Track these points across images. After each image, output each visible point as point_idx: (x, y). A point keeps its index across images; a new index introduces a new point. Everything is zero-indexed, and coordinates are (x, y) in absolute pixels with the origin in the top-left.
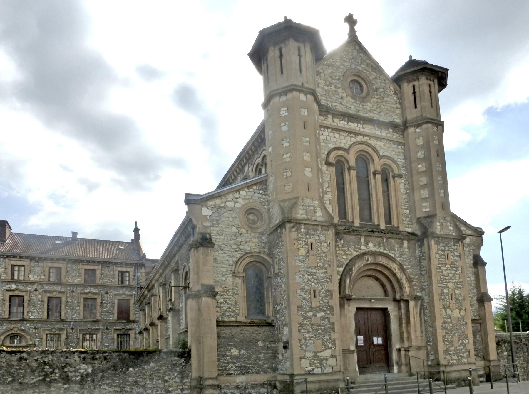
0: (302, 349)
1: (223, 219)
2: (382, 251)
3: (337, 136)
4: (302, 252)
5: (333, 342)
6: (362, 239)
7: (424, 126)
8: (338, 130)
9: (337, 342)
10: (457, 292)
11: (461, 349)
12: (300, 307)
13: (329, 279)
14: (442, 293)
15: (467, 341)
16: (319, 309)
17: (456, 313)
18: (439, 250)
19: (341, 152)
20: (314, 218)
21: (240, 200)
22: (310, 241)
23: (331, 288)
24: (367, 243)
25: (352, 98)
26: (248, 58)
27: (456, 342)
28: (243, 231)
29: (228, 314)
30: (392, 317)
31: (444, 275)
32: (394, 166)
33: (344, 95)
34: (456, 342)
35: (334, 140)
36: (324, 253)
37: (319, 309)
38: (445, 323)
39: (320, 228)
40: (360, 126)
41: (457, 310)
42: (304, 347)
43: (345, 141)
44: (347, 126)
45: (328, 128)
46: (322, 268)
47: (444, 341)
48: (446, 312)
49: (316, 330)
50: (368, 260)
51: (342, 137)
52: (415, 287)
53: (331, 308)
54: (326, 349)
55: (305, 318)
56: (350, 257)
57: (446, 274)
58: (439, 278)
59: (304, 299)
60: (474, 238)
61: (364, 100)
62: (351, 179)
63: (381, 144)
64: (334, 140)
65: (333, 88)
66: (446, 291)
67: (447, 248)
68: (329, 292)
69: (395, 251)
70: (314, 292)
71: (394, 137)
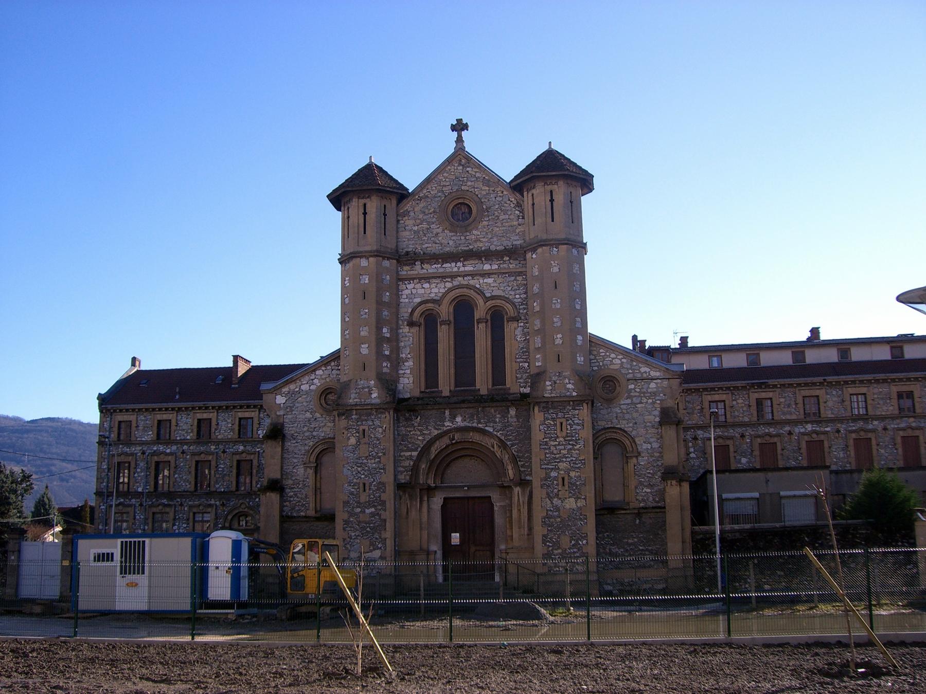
0: (347, 549)
1: (297, 405)
2: (475, 425)
3: (426, 285)
4: (353, 441)
5: (384, 541)
6: (447, 412)
7: (540, 250)
8: (427, 278)
9: (388, 542)
10: (572, 474)
11: (574, 552)
12: (346, 503)
13: (383, 469)
14: (547, 477)
15: (584, 542)
16: (370, 504)
17: (571, 504)
18: (546, 419)
19: (430, 306)
20: (368, 401)
21: (316, 381)
22: (361, 428)
23: (384, 478)
24: (453, 418)
25: (451, 231)
26: (96, 403)
27: (565, 541)
28: (318, 415)
29: (297, 508)
30: (496, 508)
31: (552, 453)
32: (508, 307)
33: (440, 230)
34: (565, 541)
35: (421, 291)
36: (378, 440)
37: (370, 504)
38: (548, 517)
39: (374, 412)
40: (459, 264)
41: (572, 500)
42: (348, 546)
43: (435, 290)
44: (441, 270)
45: (413, 279)
46: (374, 458)
47: (544, 542)
48: (552, 503)
49: (364, 528)
50: (453, 439)
51: (433, 285)
52: (522, 469)
53: (383, 503)
54: (374, 549)
55: (351, 514)
56: (428, 438)
57: (555, 452)
58: (543, 457)
59: (352, 493)
60: (666, 382)
61: (466, 229)
62: (445, 337)
63: (490, 281)
64: (422, 291)
65: (425, 226)
66: (553, 474)
67: (560, 415)
68: (382, 486)
69: (495, 422)
70: (364, 484)
71: (511, 266)
